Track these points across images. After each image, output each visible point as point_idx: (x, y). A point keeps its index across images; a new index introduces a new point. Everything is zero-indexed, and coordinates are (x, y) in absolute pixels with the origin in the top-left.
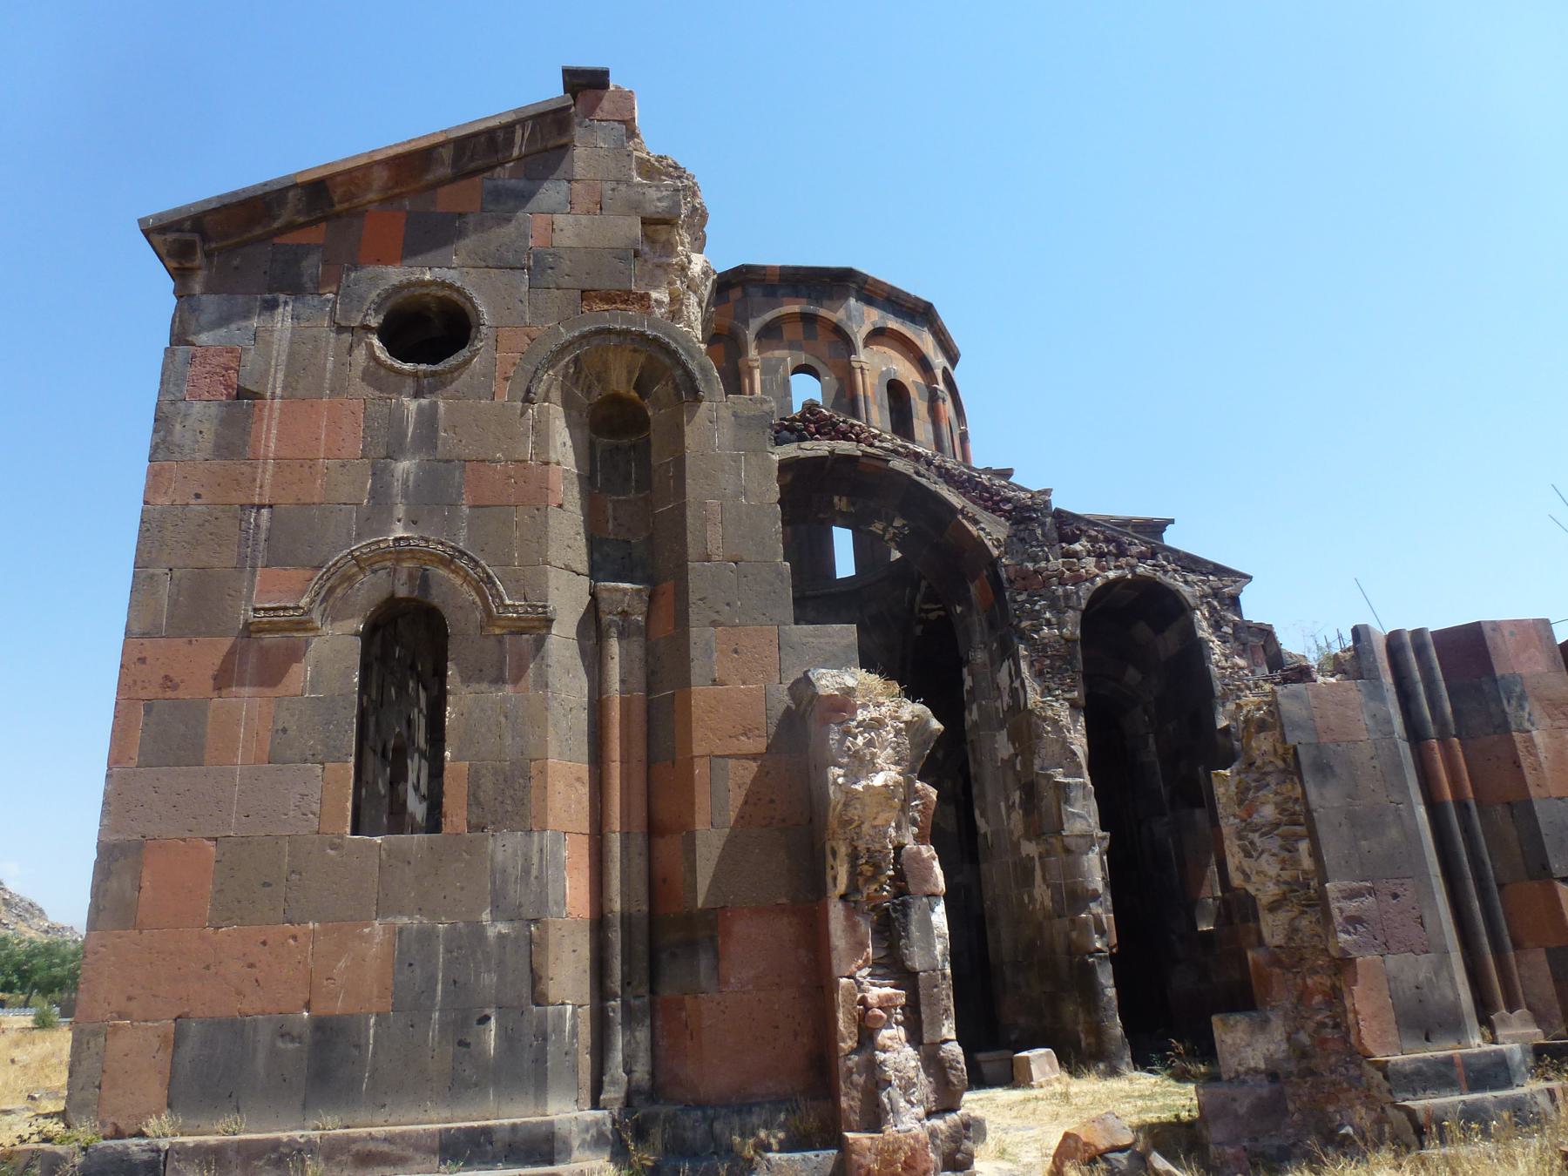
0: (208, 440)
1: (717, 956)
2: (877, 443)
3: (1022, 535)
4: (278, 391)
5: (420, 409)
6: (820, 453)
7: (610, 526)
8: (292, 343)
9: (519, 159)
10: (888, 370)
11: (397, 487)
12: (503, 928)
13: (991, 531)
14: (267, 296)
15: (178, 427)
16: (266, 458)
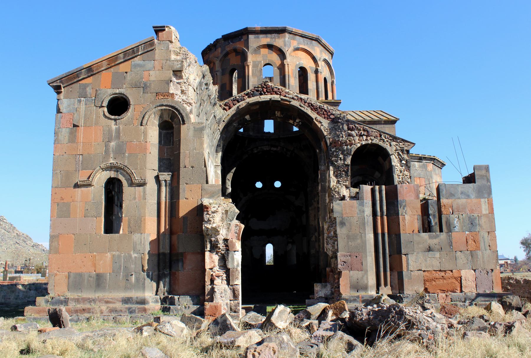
0: (67, 138)
1: (183, 263)
2: (287, 95)
3: (336, 127)
4: (83, 125)
5: (116, 128)
6: (267, 100)
7: (165, 155)
8: (85, 111)
9: (141, 54)
10: (299, 64)
11: (111, 150)
12: (136, 255)
13: (324, 125)
14: (79, 99)
15: (60, 135)
16: (80, 142)
